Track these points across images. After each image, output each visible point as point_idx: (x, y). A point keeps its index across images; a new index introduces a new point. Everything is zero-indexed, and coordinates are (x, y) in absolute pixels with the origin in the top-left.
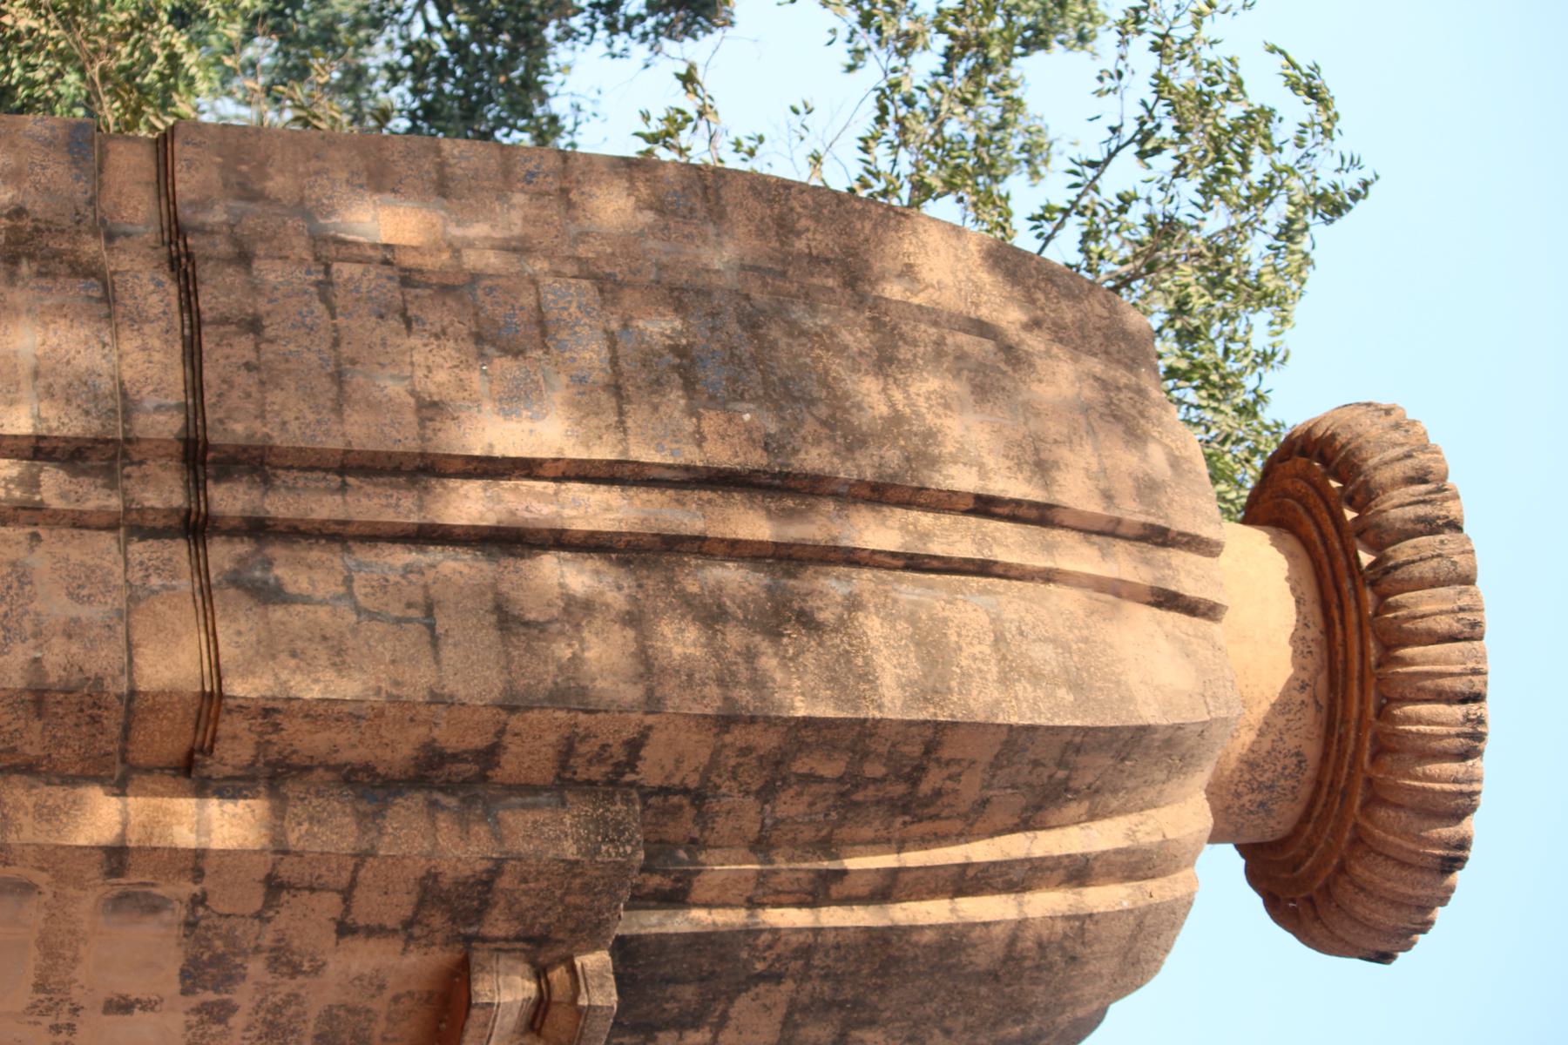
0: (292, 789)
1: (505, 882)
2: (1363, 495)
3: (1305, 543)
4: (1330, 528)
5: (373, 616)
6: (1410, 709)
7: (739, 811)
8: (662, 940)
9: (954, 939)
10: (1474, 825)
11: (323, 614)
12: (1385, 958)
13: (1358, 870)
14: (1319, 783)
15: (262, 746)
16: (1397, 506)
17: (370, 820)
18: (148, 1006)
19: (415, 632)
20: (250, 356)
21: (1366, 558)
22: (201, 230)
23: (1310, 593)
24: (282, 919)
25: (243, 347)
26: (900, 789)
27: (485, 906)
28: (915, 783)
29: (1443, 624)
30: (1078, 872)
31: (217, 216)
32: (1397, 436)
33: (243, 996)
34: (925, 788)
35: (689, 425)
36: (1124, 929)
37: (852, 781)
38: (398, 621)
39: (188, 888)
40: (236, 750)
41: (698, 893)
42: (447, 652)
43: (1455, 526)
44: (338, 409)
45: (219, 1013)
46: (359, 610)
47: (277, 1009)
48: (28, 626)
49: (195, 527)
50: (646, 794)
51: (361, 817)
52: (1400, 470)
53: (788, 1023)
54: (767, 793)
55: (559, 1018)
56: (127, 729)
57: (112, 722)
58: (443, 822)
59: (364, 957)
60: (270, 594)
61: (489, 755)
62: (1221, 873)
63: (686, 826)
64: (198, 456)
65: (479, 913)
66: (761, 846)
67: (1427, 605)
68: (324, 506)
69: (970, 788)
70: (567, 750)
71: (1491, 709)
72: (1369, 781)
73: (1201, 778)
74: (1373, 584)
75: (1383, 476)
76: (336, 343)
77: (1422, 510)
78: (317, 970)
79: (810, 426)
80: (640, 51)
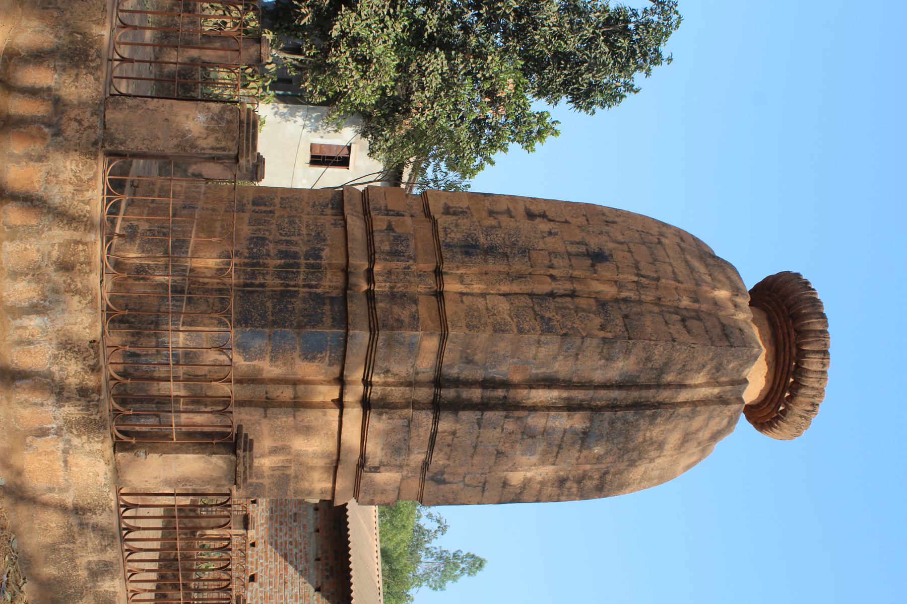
4: (781, 388)
5: (468, 486)
11: (455, 486)
20: (450, 442)
42: (486, 494)
44: (472, 456)
48: (371, 492)
76: (478, 437)
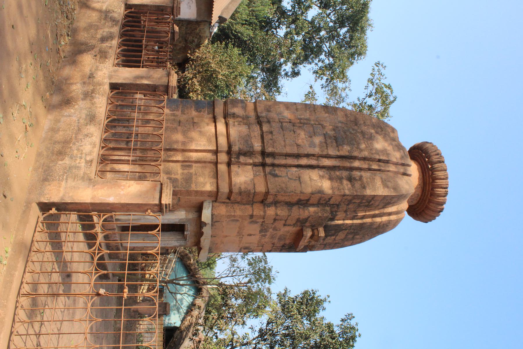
0: (278, 205)
1: (310, 219)
2: (429, 157)
3: (419, 163)
4: (423, 161)
5: (291, 179)
6: (437, 189)
7: (343, 207)
8: (331, 225)
9: (372, 224)
10: (444, 206)
11: (283, 179)
12: (426, 222)
13: (426, 211)
14: (420, 199)
15: (274, 199)
16: (435, 159)
17: (290, 210)
18: (254, 235)
19: (297, 182)
21: (430, 166)
22: (261, 117)
23: (420, 170)
24: (276, 224)
25: (270, 136)
26: (367, 204)
27: (306, 222)
28: (369, 202)
29: (442, 177)
30: (390, 214)
31: (264, 115)
32: (433, 148)
33: (268, 234)
34: (371, 204)
35: (337, 149)
36: (395, 222)
37: (361, 203)
38: (295, 180)
39: (262, 220)
40: (270, 199)
41: (336, 218)
43: (443, 162)
45: (264, 236)
46: (289, 178)
47: (273, 235)
49: (263, 165)
50: (330, 205)
51: (289, 210)
52: (434, 153)
53: (346, 235)
54: (348, 205)
55: (316, 237)
56: (253, 197)
57: (251, 196)
58: (301, 210)
59: (287, 228)
60: (275, 176)
61: (308, 200)
62: (406, 213)
63: (336, 209)
64: (263, 153)
65: (305, 223)
66: (346, 211)
67: (440, 174)
68: (283, 161)
69: (377, 204)
70: (320, 199)
71: (449, 189)
72: (429, 199)
73: (407, 200)
74: (431, 170)
75: (432, 154)
76: (284, 135)
77: (439, 160)
78: (280, 230)
79: (354, 148)
80: (290, 79)
